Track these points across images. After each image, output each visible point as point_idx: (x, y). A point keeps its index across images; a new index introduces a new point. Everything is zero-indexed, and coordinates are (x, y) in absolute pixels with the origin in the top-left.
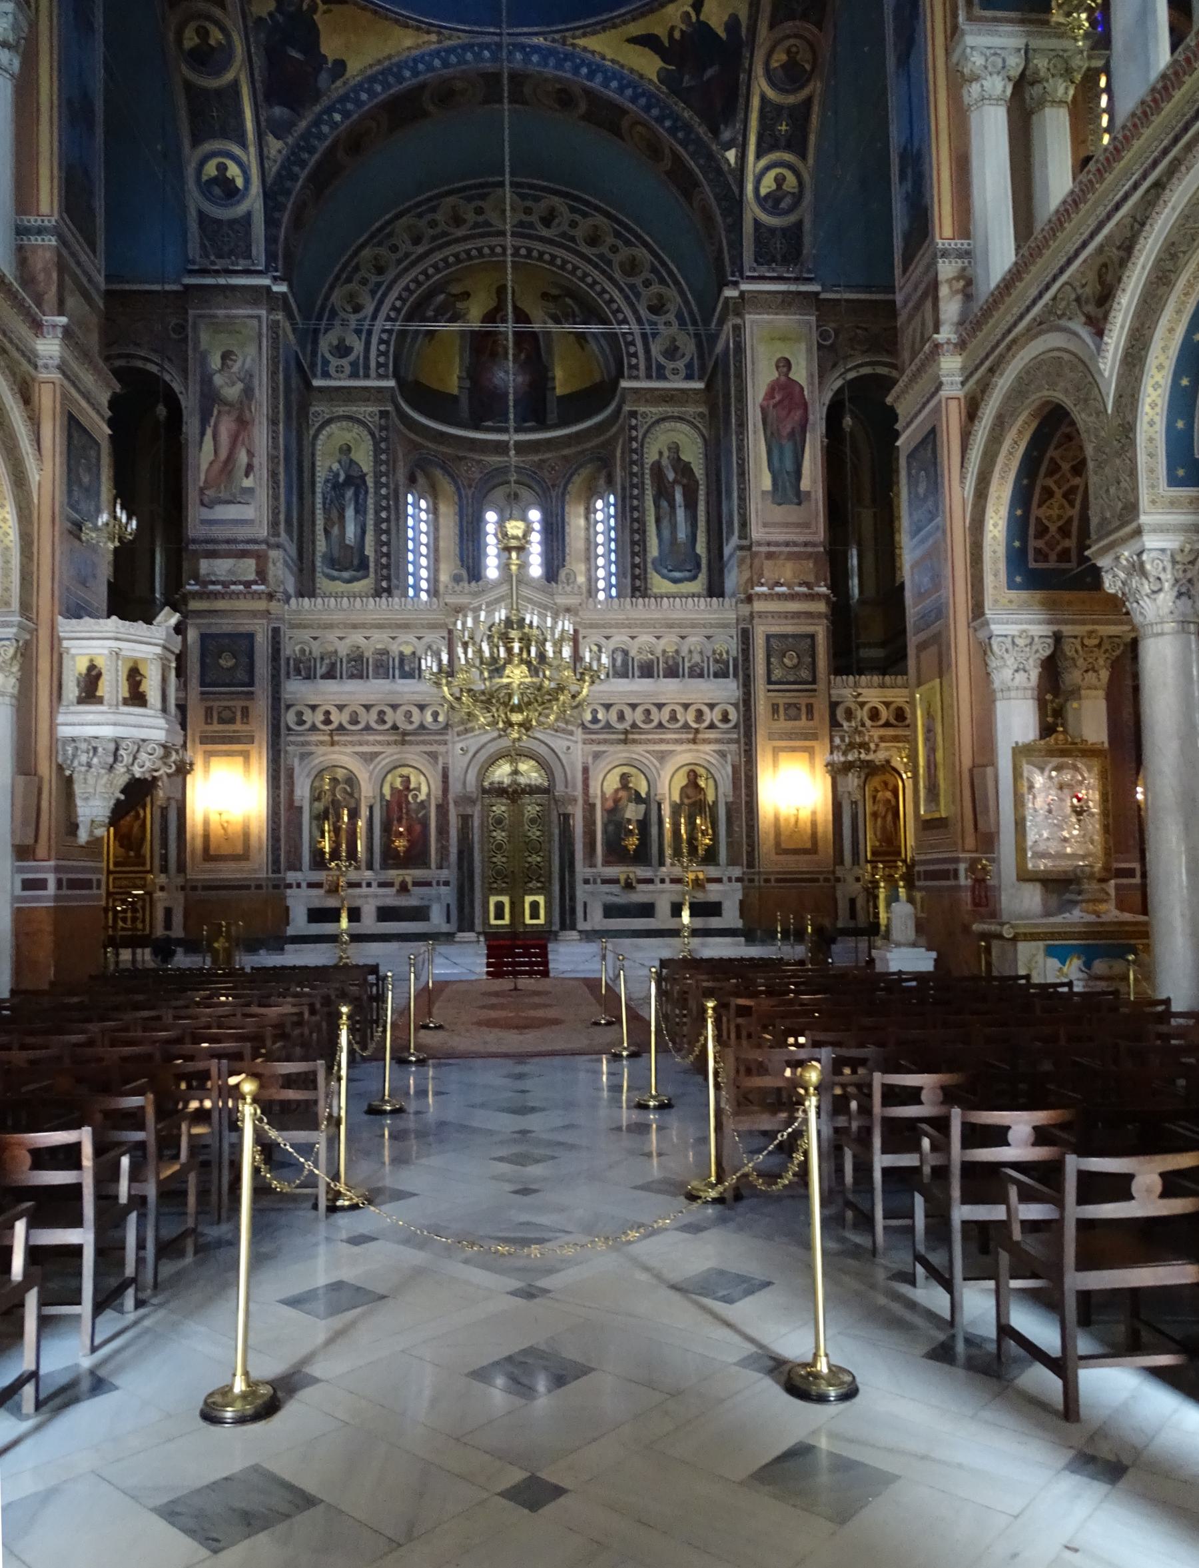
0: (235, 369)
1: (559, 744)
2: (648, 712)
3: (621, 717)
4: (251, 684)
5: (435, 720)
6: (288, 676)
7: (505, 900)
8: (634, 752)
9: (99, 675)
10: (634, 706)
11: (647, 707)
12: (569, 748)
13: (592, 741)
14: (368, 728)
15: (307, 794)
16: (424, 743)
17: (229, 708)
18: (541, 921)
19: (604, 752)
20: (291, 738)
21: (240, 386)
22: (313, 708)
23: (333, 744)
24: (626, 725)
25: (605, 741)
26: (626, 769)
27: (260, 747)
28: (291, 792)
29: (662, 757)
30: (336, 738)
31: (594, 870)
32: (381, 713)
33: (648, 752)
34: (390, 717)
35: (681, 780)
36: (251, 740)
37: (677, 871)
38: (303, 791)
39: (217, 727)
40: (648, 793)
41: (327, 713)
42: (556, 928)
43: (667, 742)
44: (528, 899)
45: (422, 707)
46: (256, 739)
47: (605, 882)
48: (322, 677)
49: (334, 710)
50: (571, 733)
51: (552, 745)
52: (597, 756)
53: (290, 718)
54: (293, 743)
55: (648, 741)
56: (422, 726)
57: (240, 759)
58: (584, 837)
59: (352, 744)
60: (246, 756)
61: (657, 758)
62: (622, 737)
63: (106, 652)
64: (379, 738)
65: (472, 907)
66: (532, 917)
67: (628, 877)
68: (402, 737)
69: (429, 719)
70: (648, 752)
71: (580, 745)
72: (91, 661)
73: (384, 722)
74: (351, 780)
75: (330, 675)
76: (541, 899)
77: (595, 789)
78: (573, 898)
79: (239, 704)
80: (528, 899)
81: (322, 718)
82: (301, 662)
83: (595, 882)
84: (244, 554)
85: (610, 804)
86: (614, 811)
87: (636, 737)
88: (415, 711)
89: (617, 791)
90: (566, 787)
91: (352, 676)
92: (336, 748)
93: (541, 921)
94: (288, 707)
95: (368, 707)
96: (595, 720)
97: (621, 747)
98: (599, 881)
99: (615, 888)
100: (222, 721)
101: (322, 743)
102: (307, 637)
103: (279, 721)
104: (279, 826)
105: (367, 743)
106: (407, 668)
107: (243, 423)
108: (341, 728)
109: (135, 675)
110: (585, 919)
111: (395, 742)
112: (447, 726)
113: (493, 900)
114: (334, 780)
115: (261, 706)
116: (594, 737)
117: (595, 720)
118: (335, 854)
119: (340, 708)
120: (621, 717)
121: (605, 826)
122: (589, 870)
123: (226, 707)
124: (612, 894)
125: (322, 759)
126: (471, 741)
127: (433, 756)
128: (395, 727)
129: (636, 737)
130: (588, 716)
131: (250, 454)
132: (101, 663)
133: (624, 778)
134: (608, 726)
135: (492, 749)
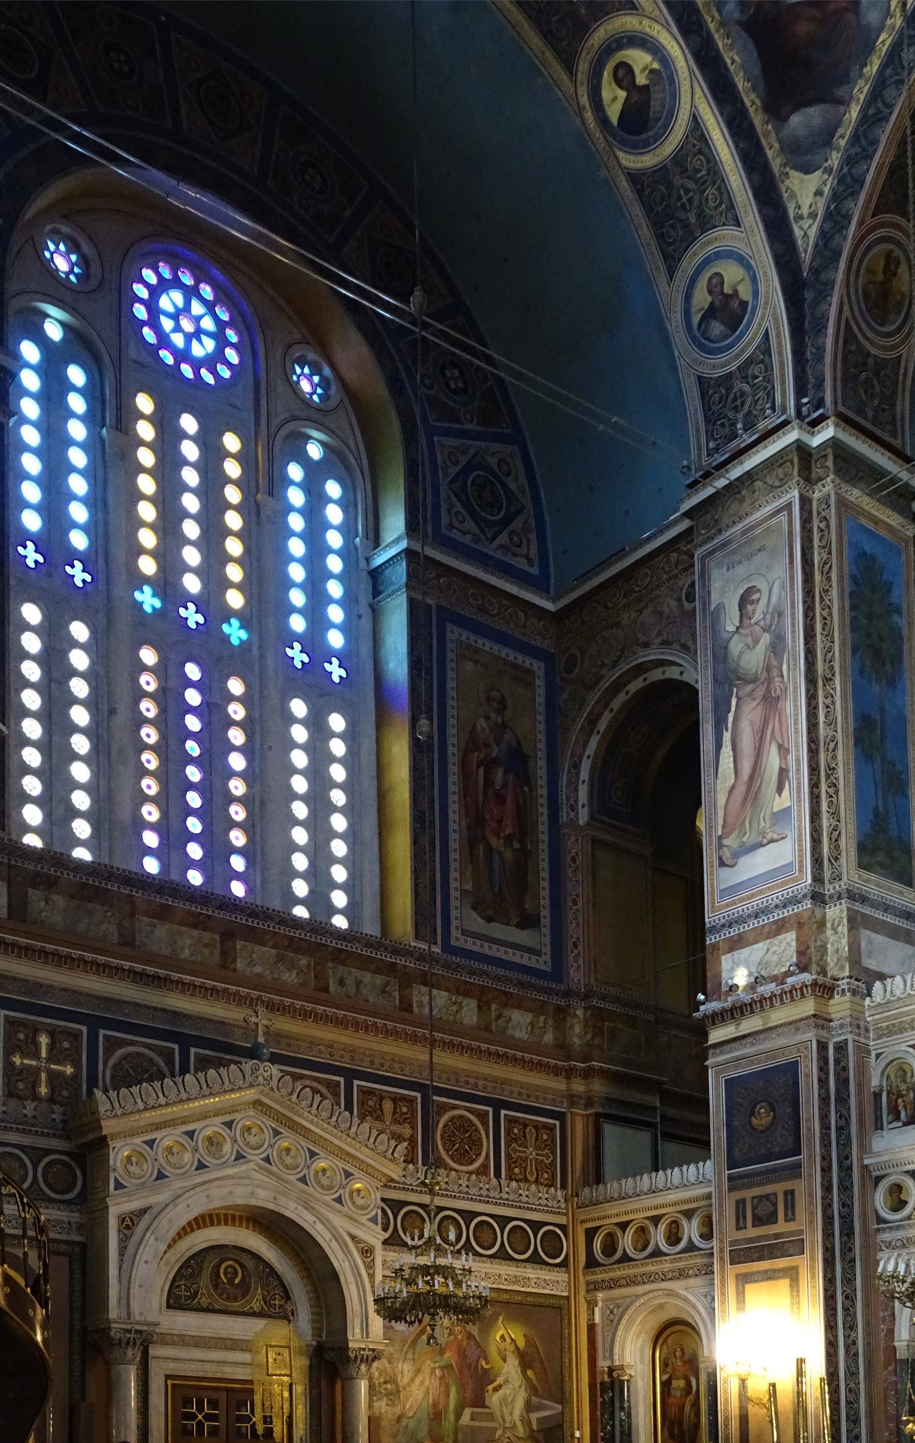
0: (758, 616)
6: (879, 1126)
17: (767, 1197)
20: (887, 1236)
21: (766, 639)
27: (812, 1259)
36: (798, 1247)
39: (751, 1232)
57: (784, 1284)
60: (792, 1275)
79: (779, 1188)
82: (899, 1095)
84: (780, 927)
100: (759, 1221)
102: (903, 1047)
104: (857, 1394)
107: (771, 702)
123: (761, 1198)
131: (783, 750)
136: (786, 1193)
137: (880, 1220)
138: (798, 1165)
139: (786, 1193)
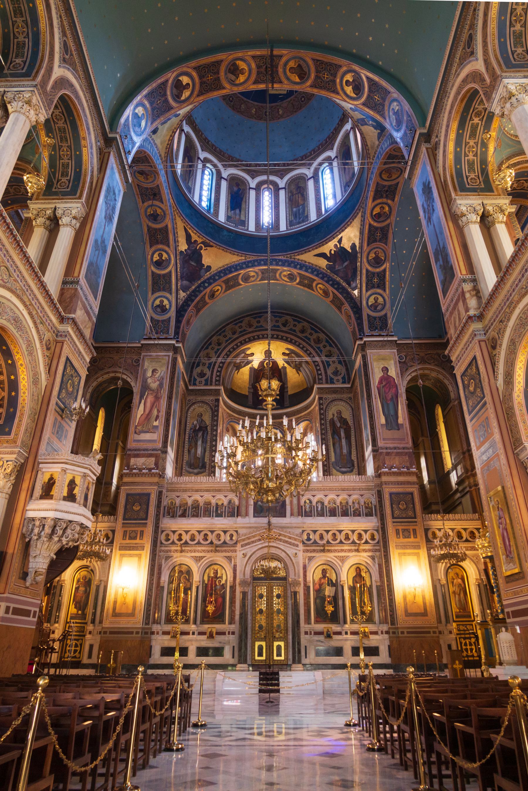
1: (291, 551)
2: (334, 535)
3: (321, 537)
4: (146, 519)
5: (231, 539)
7: (263, 644)
8: (328, 557)
9: (54, 483)
10: (327, 532)
11: (333, 532)
12: (296, 554)
13: (308, 551)
14: (199, 543)
15: (167, 580)
16: (225, 551)
18: (282, 658)
19: (314, 557)
20: (163, 548)
22: (174, 532)
23: (182, 551)
24: (324, 542)
25: (314, 551)
26: (325, 567)
28: (159, 578)
29: (343, 560)
30: (183, 548)
31: (310, 626)
32: (206, 535)
33: (336, 557)
34: (210, 537)
35: (353, 573)
36: (143, 548)
37: (355, 627)
38: (165, 578)
40: (336, 580)
41: (180, 535)
42: (290, 662)
43: (345, 551)
44: (276, 644)
45: (225, 532)
46: (145, 548)
47: (316, 633)
48: (180, 516)
49: (184, 534)
50: (297, 546)
51: (288, 552)
52: (310, 559)
53: (163, 537)
54: (163, 551)
55: (335, 551)
56: (225, 542)
57: (136, 559)
58: (305, 606)
59: (191, 551)
60: (139, 556)
61: (340, 560)
62: (322, 548)
63: (59, 470)
64: (203, 548)
65: (246, 649)
66: (277, 656)
67: (328, 631)
68: (216, 548)
69: (229, 538)
70: (336, 557)
71: (301, 552)
72: (52, 475)
73: (207, 540)
74: (189, 572)
75: (183, 515)
76: (282, 644)
77: (310, 578)
78: (299, 644)
80: (276, 644)
81: (178, 537)
83: (311, 634)
85: (317, 586)
86: (319, 591)
87: (329, 548)
88: (222, 534)
89: (320, 579)
90: (295, 575)
91: (193, 516)
92: (183, 554)
93: (282, 658)
94: (163, 531)
95: (199, 532)
96: (309, 539)
97: (322, 554)
98: (313, 633)
99: (321, 638)
101: (176, 551)
103: (157, 538)
105: (198, 551)
106: (219, 512)
108: (186, 543)
109: (72, 484)
110: (306, 657)
111: (211, 551)
112: (236, 543)
113: (257, 644)
114: (180, 572)
115: (149, 530)
116: (308, 548)
117: (309, 539)
118: (177, 613)
119: (187, 532)
120: (321, 537)
121: (315, 600)
122: (307, 626)
124: (319, 641)
125: (175, 560)
126: (248, 550)
127: (229, 558)
128: (212, 543)
129: (329, 548)
130: (305, 537)
132: (56, 477)
133: (324, 572)
134: (315, 542)
135: (259, 554)
136: (141, 531)
137: (161, 543)
138: (146, 523)
139: (141, 531)
